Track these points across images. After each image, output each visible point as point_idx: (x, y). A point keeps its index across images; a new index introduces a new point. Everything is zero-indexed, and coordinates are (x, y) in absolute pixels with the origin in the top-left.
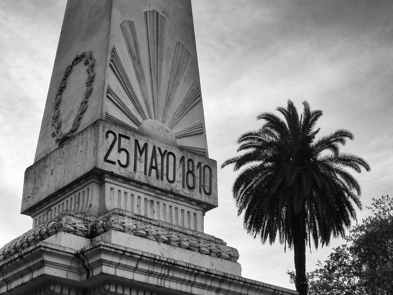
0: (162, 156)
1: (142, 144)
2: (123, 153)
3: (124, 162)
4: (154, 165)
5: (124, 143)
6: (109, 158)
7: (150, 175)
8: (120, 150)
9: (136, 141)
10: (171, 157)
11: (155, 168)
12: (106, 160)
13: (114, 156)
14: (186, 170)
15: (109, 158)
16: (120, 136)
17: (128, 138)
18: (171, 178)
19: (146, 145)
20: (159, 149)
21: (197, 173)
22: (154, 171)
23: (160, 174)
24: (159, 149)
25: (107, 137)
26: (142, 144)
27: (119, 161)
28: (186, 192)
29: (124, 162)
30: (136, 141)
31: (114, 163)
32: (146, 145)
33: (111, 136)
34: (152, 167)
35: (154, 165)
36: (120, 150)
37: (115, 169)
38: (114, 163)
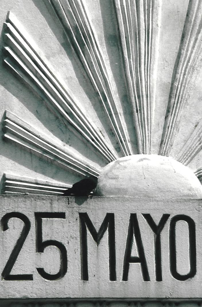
0: (157, 229)
1: (97, 223)
3: (53, 268)
4: (135, 253)
5: (51, 229)
6: (14, 272)
8: (41, 246)
9: (84, 218)
10: (182, 227)
11: (142, 259)
12: (7, 275)
13: (28, 261)
15: (14, 272)
16: (39, 216)
17: (62, 215)
18: (184, 268)
19: (110, 219)
20: (148, 217)
22: (135, 268)
24: (148, 217)
25: (5, 228)
26: (97, 223)
27: (41, 271)
29: (53, 268)
30: (84, 218)
31: (29, 277)
33: (16, 226)
34: (128, 259)
35: (135, 253)
36: (41, 246)
38: (29, 277)
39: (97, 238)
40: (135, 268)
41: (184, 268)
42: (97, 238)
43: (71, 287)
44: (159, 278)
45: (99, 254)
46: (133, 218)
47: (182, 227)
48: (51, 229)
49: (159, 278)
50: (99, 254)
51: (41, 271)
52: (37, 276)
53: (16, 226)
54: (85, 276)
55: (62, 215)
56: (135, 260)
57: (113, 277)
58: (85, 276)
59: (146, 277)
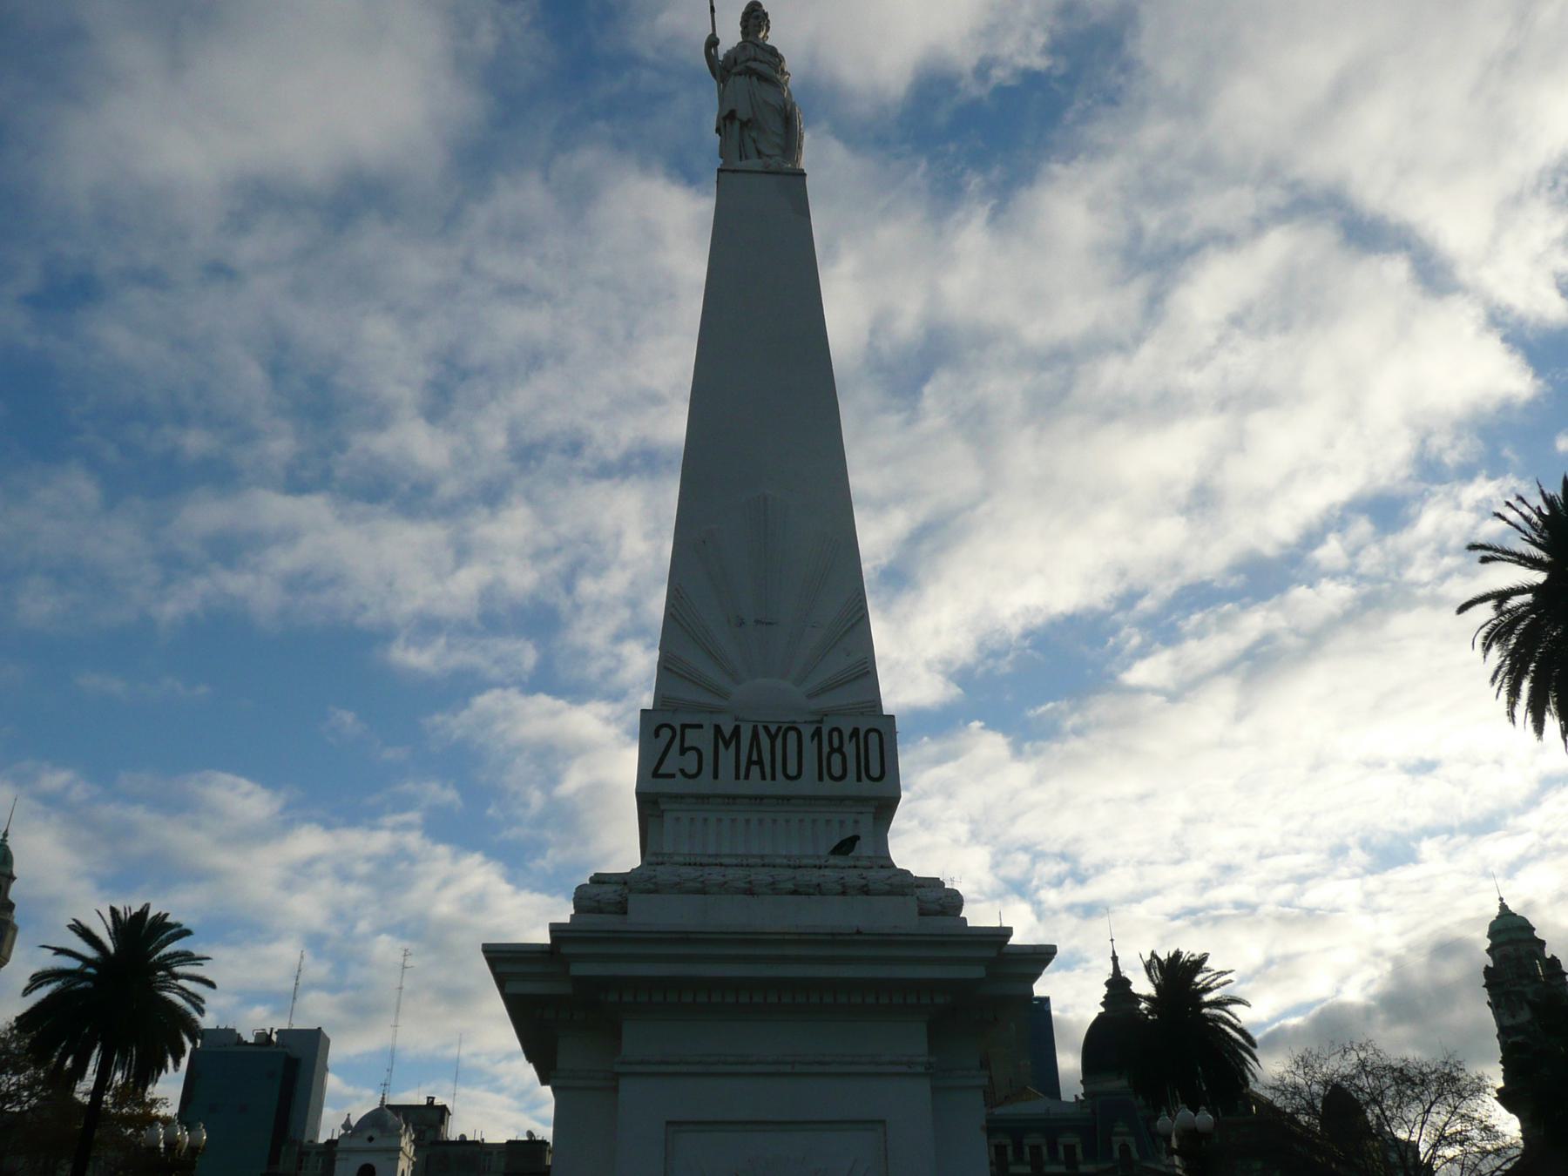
0: (773, 738)
1: (727, 731)
2: (692, 755)
4: (755, 757)
5: (692, 738)
7: (747, 777)
8: (683, 751)
9: (718, 728)
10: (792, 736)
11: (760, 762)
13: (672, 764)
14: (826, 749)
16: (684, 727)
17: (700, 726)
18: (792, 771)
19: (737, 731)
20: (766, 729)
21: (850, 749)
22: (755, 770)
23: (768, 770)
24: (766, 729)
25: (657, 734)
26: (727, 731)
27: (682, 771)
28: (829, 787)
29: (693, 769)
31: (673, 776)
32: (737, 730)
33: (666, 734)
34: (750, 762)
35: (755, 757)
36: (683, 751)
37: (679, 785)
38: (673, 776)
39: (727, 746)
40: (755, 770)
41: (792, 771)
42: (727, 746)
43: (704, 784)
44: (773, 778)
45: (727, 757)
46: (755, 727)
47: (792, 736)
48: (692, 738)
49: (773, 778)
50: (727, 757)
51: (682, 771)
52: (679, 775)
53: (666, 734)
54: (716, 776)
55: (700, 726)
56: (755, 763)
57: (737, 777)
58: (716, 776)
59: (763, 777)
